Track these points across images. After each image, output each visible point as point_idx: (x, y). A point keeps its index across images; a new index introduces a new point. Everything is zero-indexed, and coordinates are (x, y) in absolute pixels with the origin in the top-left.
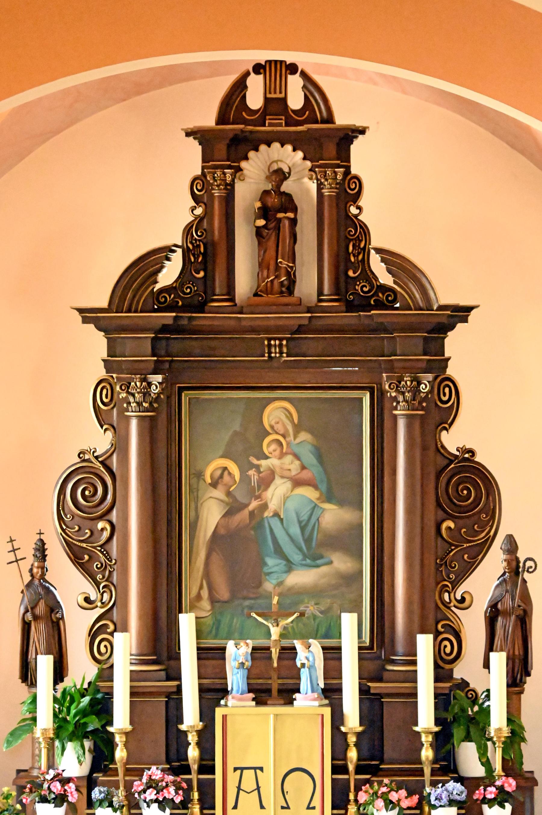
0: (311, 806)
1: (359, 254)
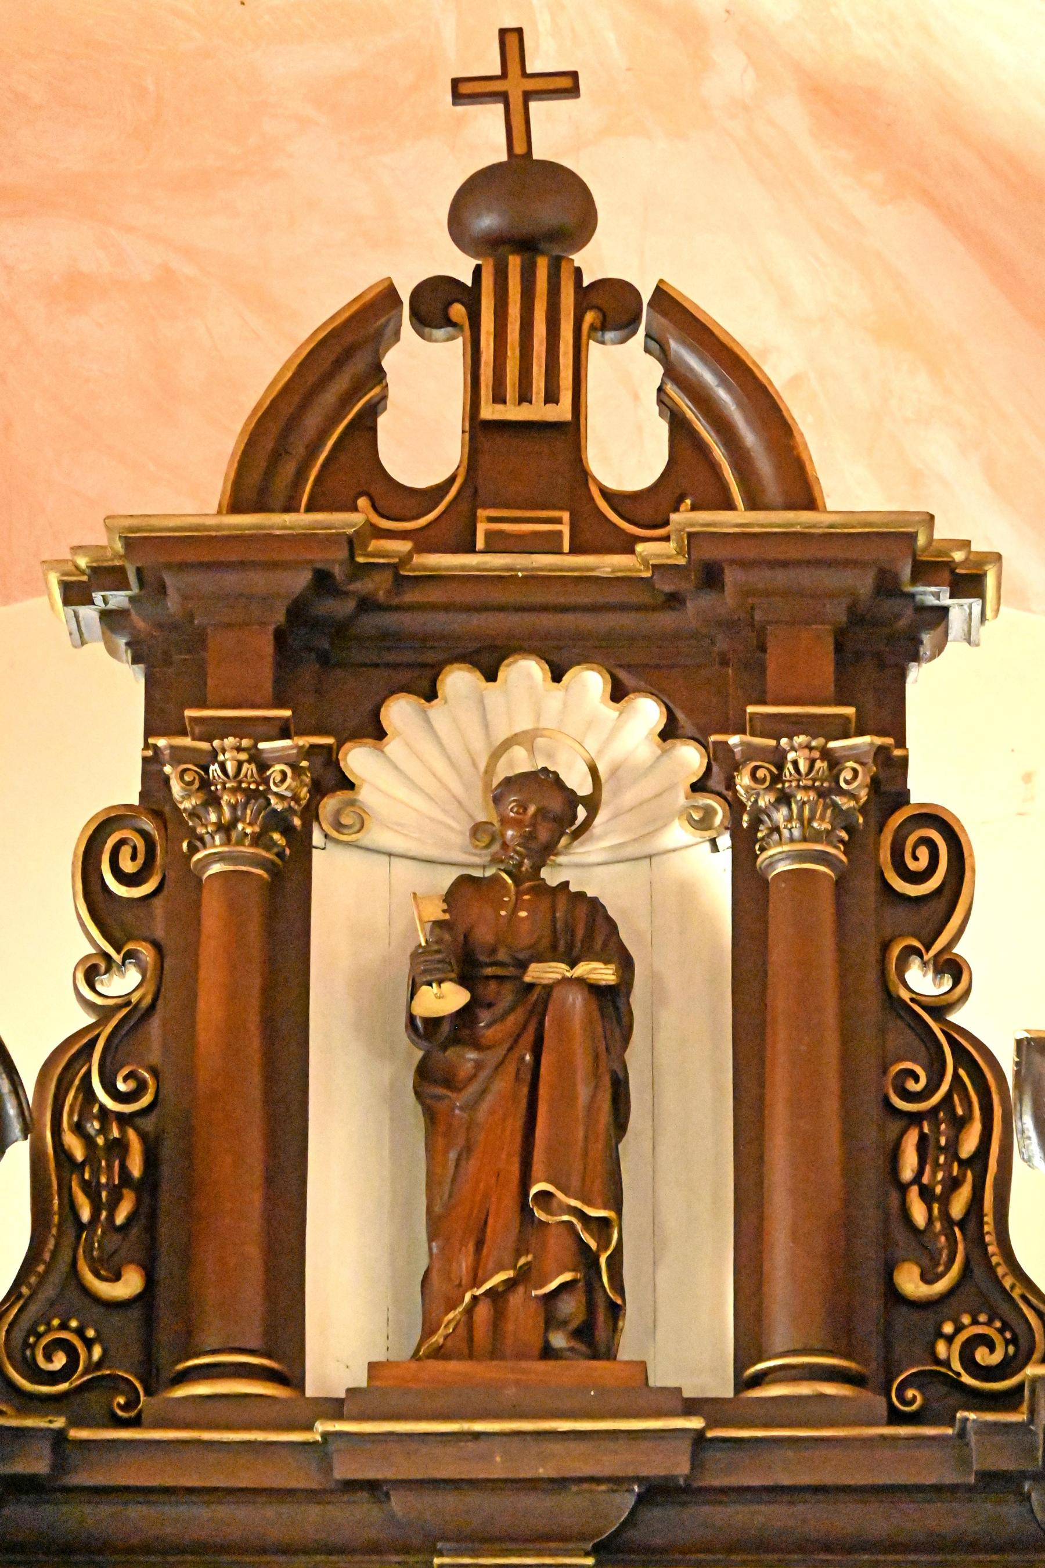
1: (953, 1184)
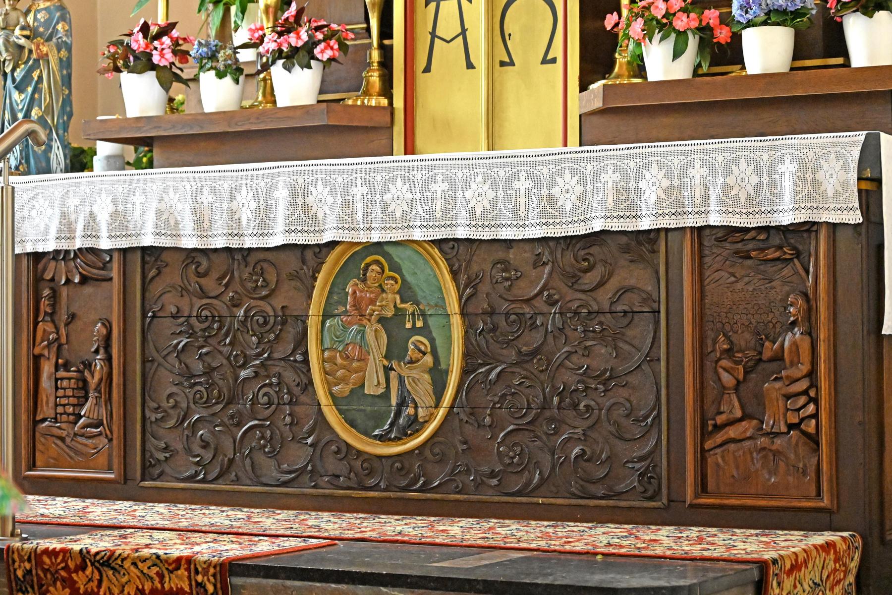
0: (549, 57)
